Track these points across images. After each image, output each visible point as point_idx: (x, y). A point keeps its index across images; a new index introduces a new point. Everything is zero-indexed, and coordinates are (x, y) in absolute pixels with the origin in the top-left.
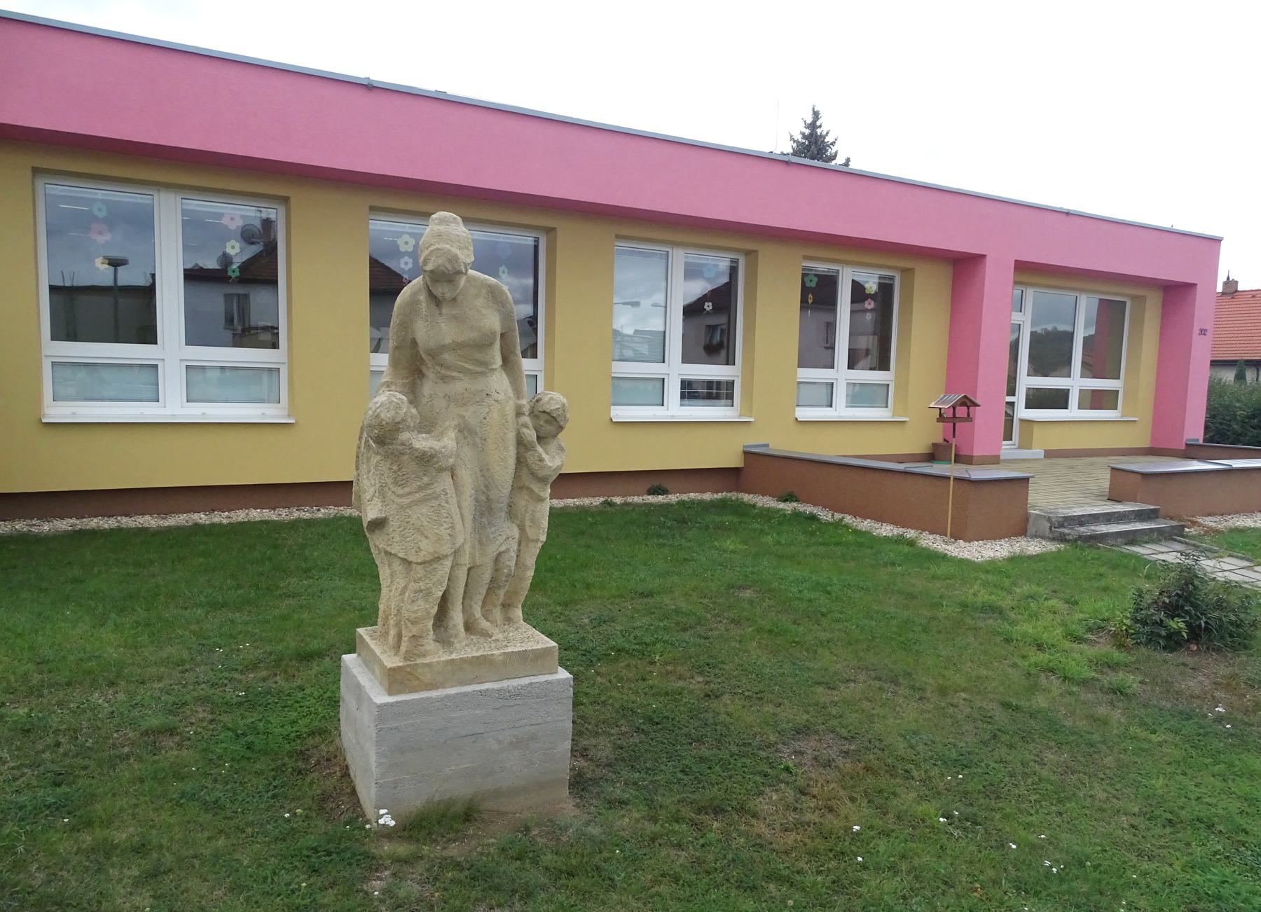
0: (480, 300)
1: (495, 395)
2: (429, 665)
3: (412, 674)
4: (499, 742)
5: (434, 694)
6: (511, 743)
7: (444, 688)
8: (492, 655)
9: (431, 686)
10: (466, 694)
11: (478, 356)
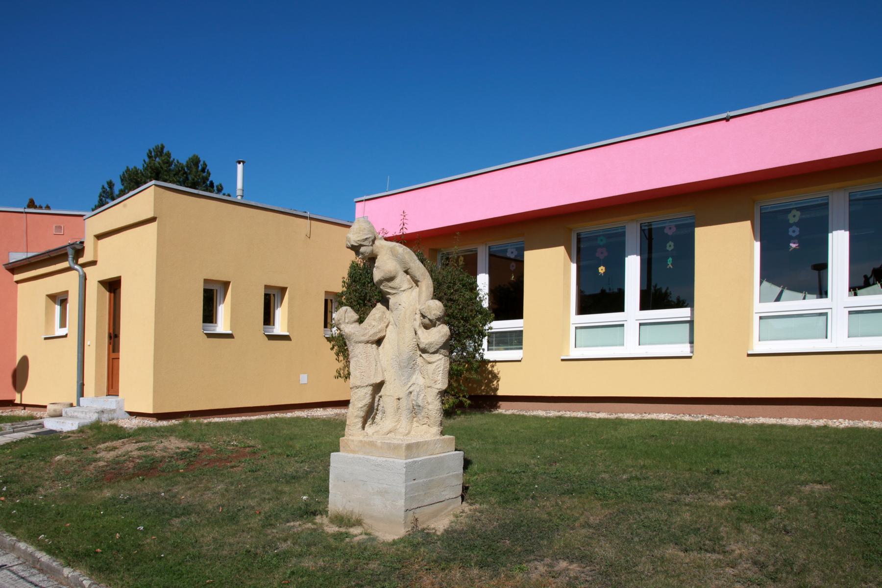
1: (403, 304)
2: (353, 441)
3: (347, 444)
4: (373, 489)
5: (351, 455)
6: (377, 491)
9: (353, 452)
10: (360, 459)
11: (391, 284)
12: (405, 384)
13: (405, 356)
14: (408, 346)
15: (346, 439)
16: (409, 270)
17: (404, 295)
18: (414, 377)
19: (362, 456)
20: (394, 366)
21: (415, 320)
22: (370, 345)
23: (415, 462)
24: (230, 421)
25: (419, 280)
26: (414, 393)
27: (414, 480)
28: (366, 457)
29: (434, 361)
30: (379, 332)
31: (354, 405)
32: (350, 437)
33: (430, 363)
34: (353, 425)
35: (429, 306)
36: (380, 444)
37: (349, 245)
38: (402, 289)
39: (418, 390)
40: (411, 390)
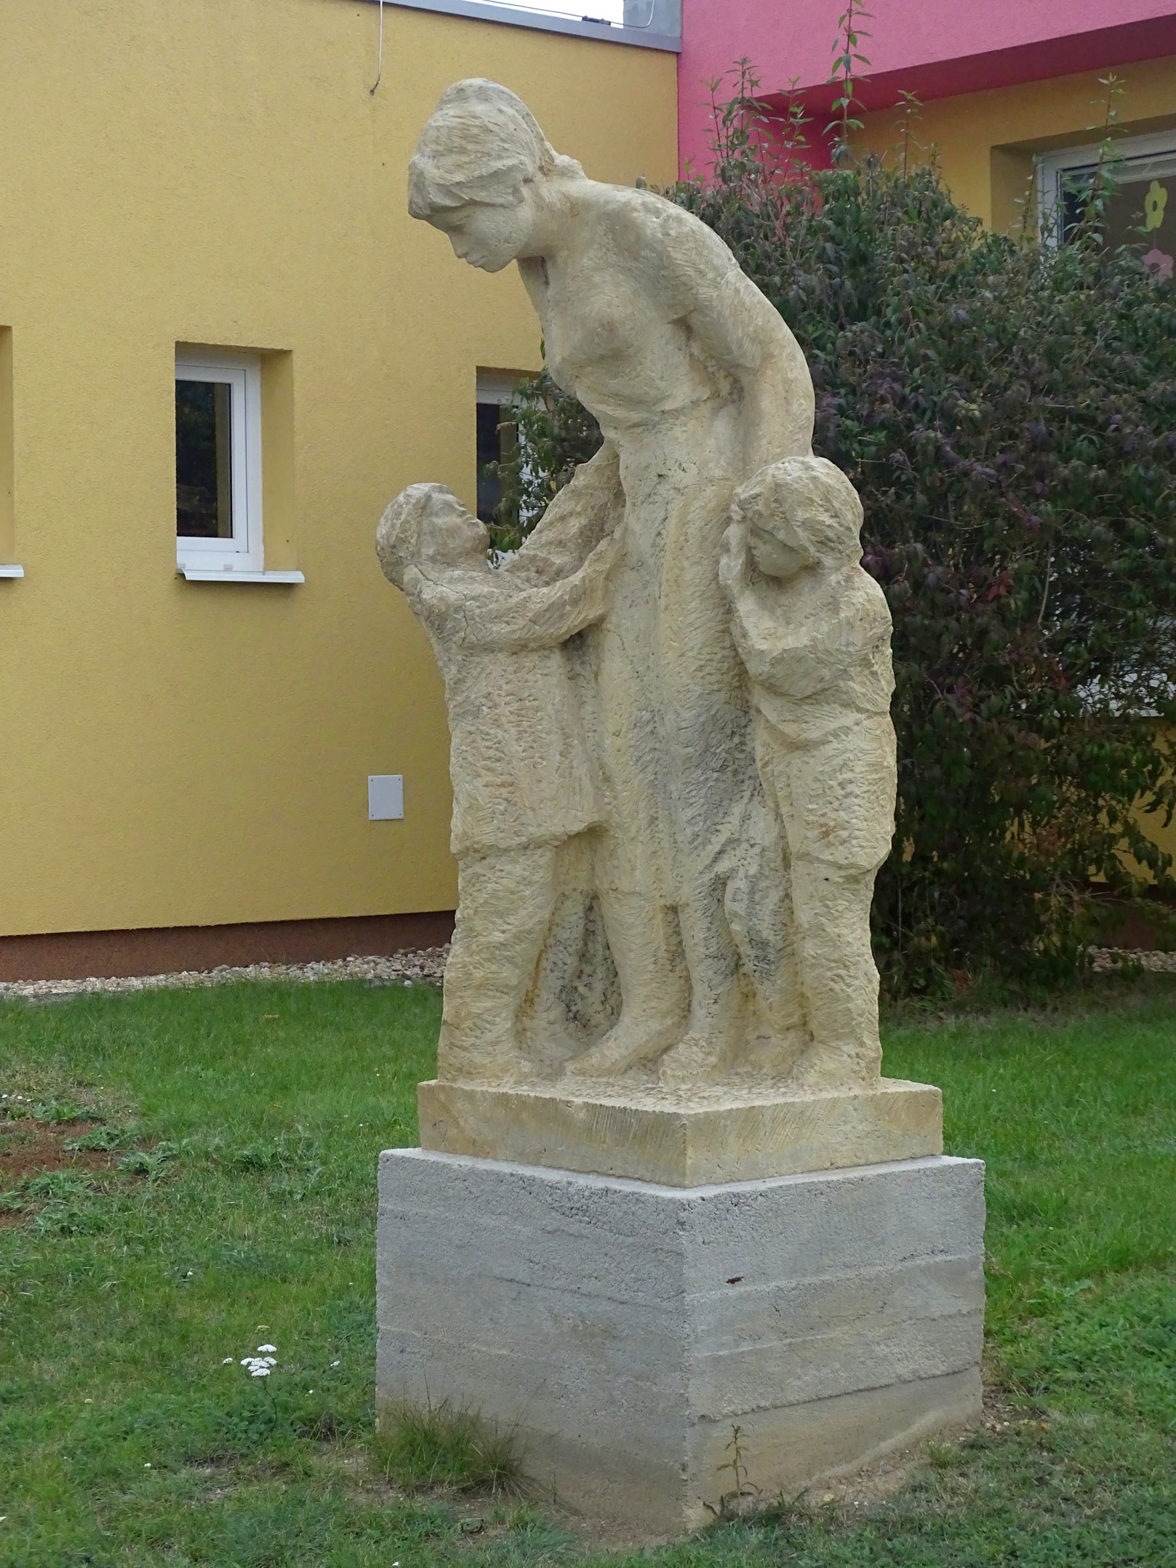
0: (592, 253)
1: (677, 476)
2: (470, 1096)
3: (448, 1111)
4: (556, 1317)
5: (464, 1162)
7: (495, 1159)
8: (568, 1103)
9: (476, 1148)
12: (698, 841)
13: (688, 715)
14: (700, 669)
15: (443, 1088)
16: (695, 320)
17: (678, 432)
18: (737, 810)
19: (505, 1168)
20: (647, 758)
21: (726, 548)
22: (535, 657)
23: (737, 1200)
24: (24, 999)
25: (741, 361)
26: (739, 884)
27: (732, 1281)
28: (527, 1171)
29: (815, 734)
30: (575, 602)
31: (471, 933)
32: (463, 1085)
33: (798, 748)
34: (469, 1023)
35: (778, 487)
36: (582, 1115)
37: (421, 203)
38: (668, 406)
39: (753, 870)
40: (723, 866)
